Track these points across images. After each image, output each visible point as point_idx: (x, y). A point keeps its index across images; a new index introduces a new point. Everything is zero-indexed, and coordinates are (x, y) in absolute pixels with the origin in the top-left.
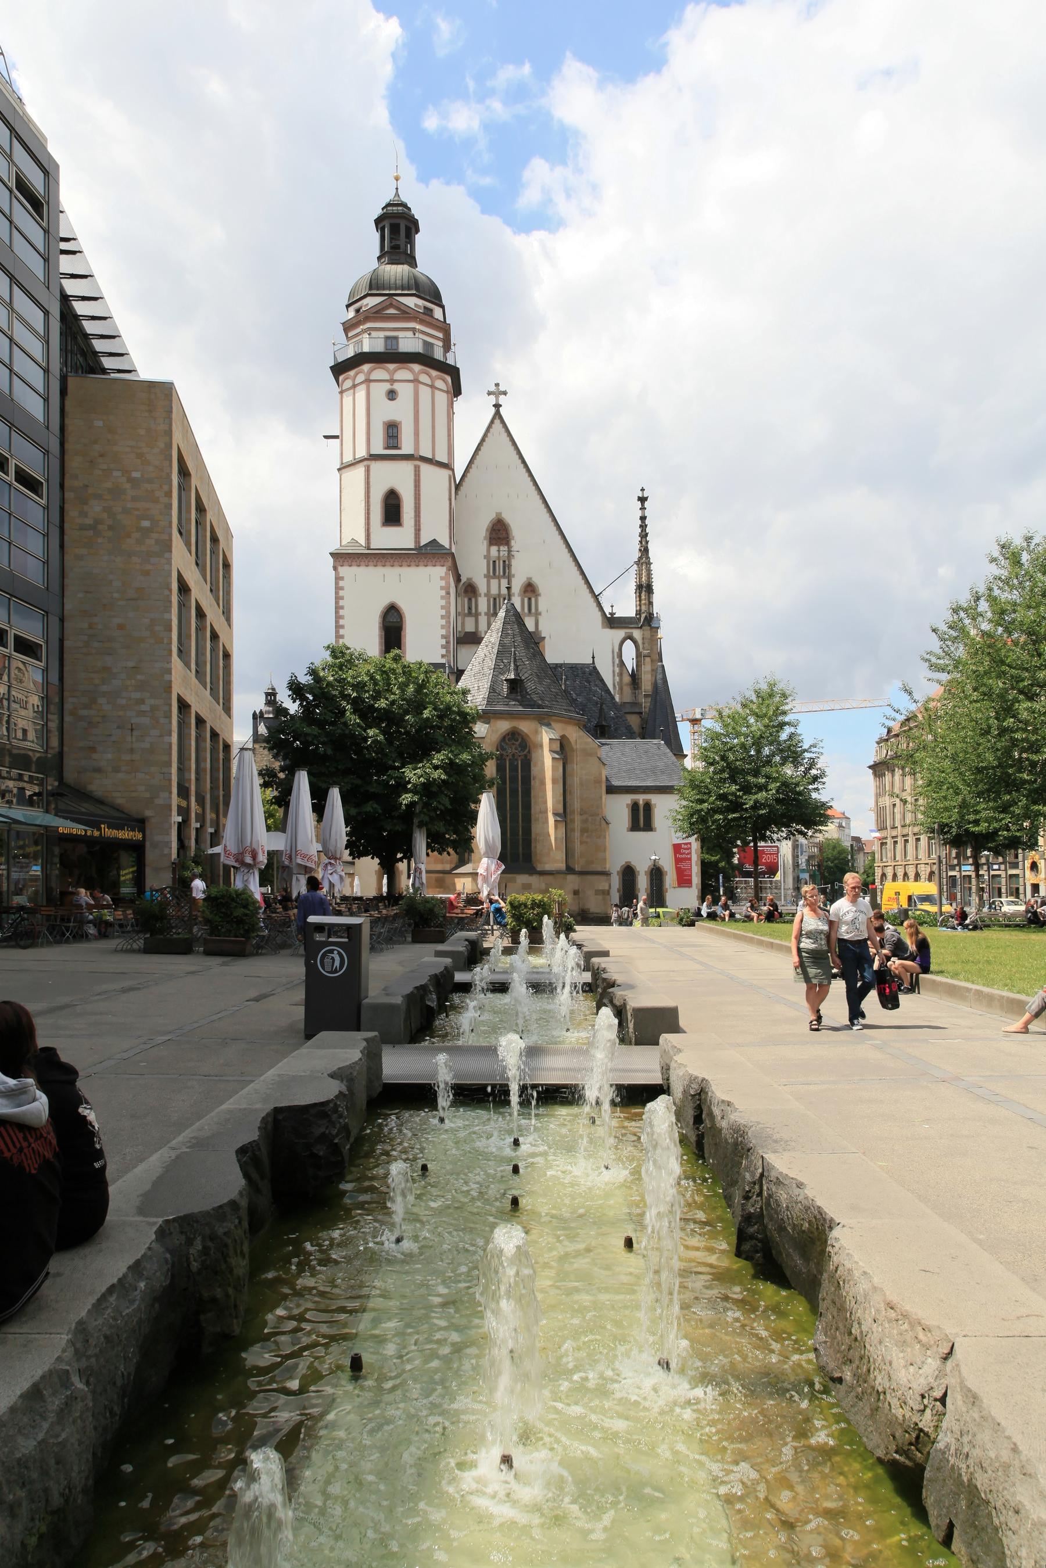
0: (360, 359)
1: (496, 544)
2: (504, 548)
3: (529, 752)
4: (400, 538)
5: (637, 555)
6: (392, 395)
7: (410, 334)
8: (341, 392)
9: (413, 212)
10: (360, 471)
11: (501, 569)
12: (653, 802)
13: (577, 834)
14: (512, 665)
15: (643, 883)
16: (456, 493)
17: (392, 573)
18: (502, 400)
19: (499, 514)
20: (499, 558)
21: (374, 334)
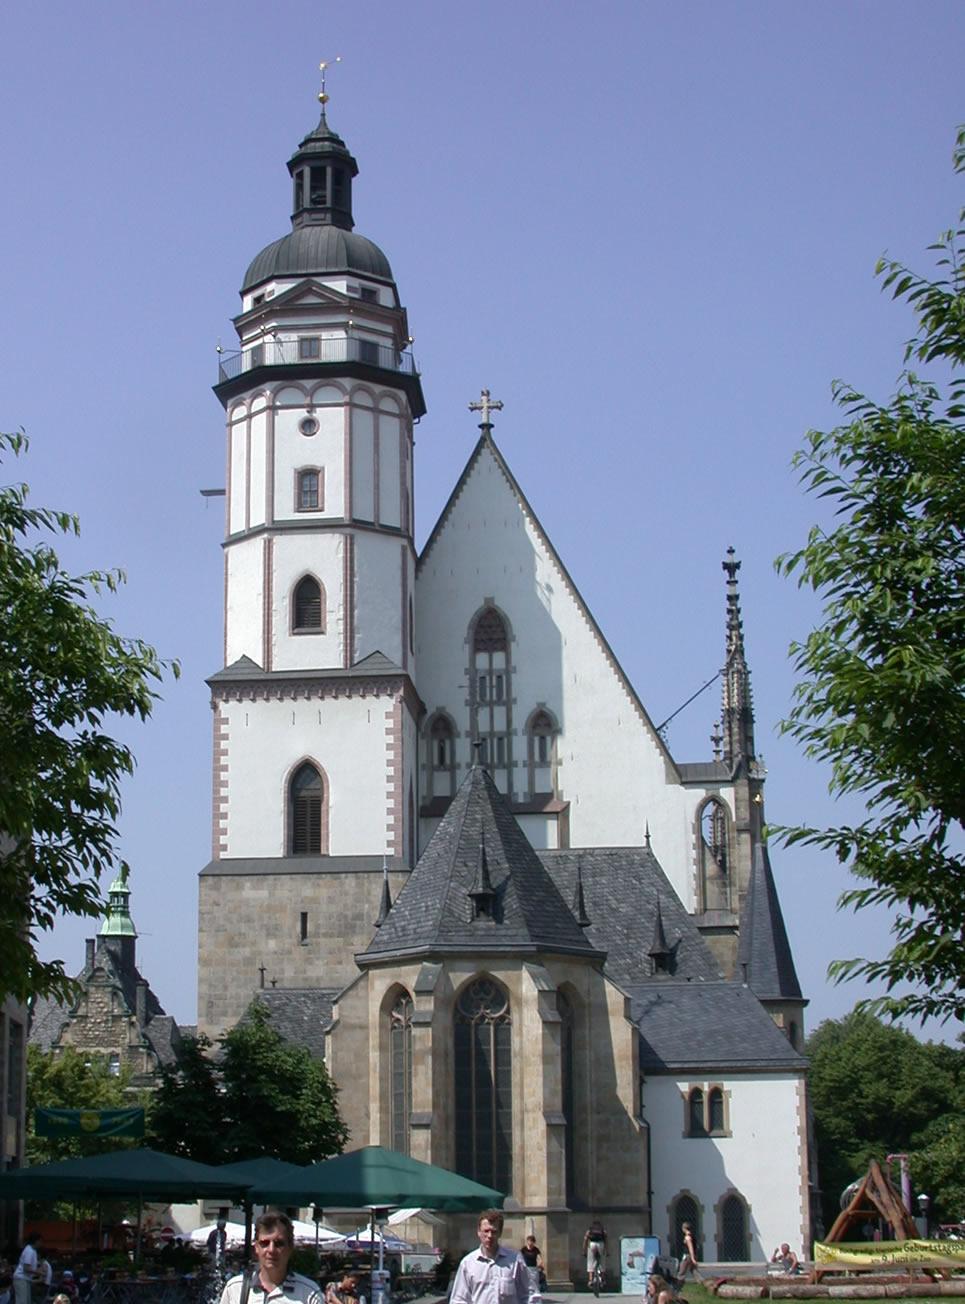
0: (261, 375)
1: (485, 650)
2: (499, 659)
3: (508, 1011)
4: (323, 652)
5: (725, 659)
6: (308, 426)
7: (341, 334)
8: (231, 424)
9: (347, 147)
10: (258, 543)
12: (725, 1089)
13: (591, 1146)
14: (480, 871)
15: (710, 1224)
16: (418, 569)
17: (305, 708)
18: (495, 417)
19: (489, 601)
20: (490, 672)
21: (281, 336)
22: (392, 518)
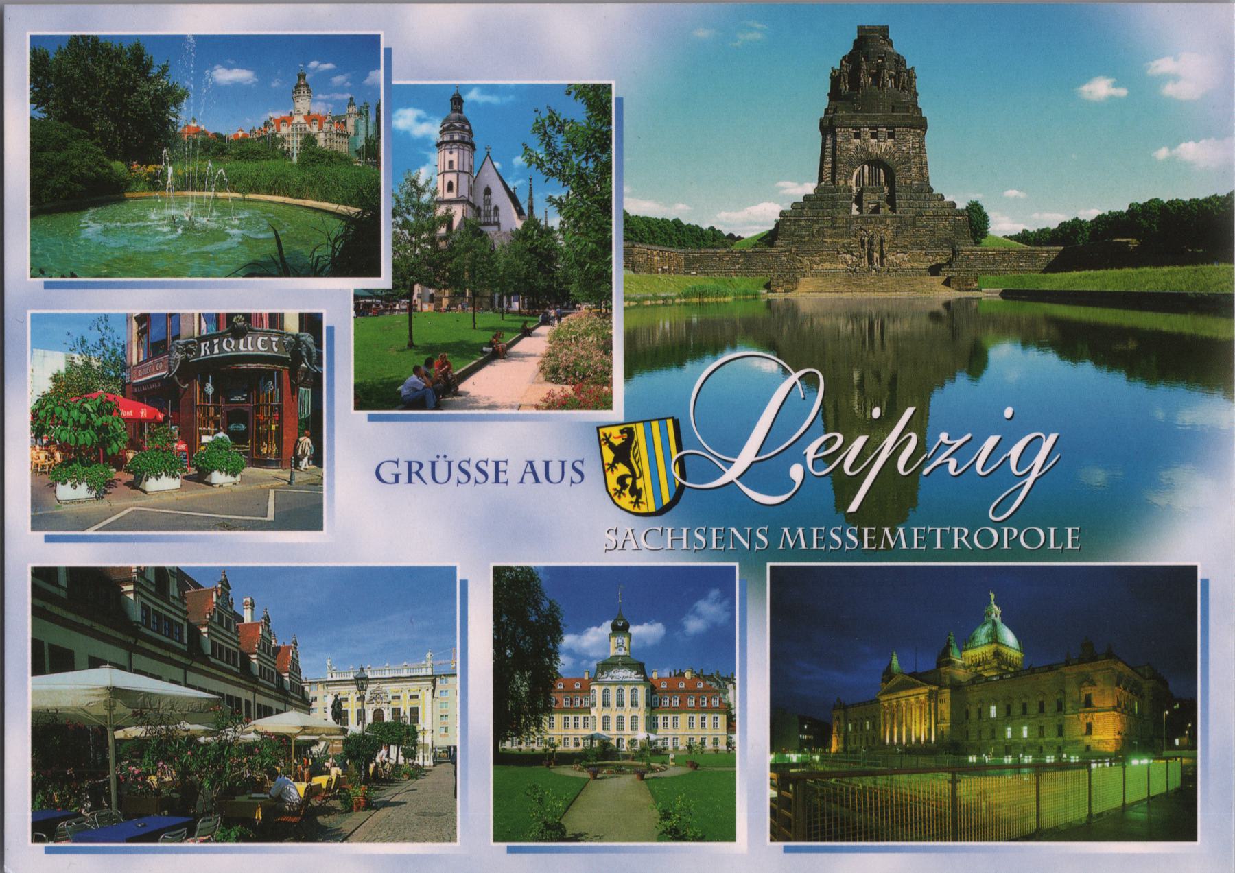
0: (443, 142)
4: (452, 195)
6: (451, 153)
10: (441, 176)
11: (488, 202)
16: (474, 181)
22: (467, 170)
